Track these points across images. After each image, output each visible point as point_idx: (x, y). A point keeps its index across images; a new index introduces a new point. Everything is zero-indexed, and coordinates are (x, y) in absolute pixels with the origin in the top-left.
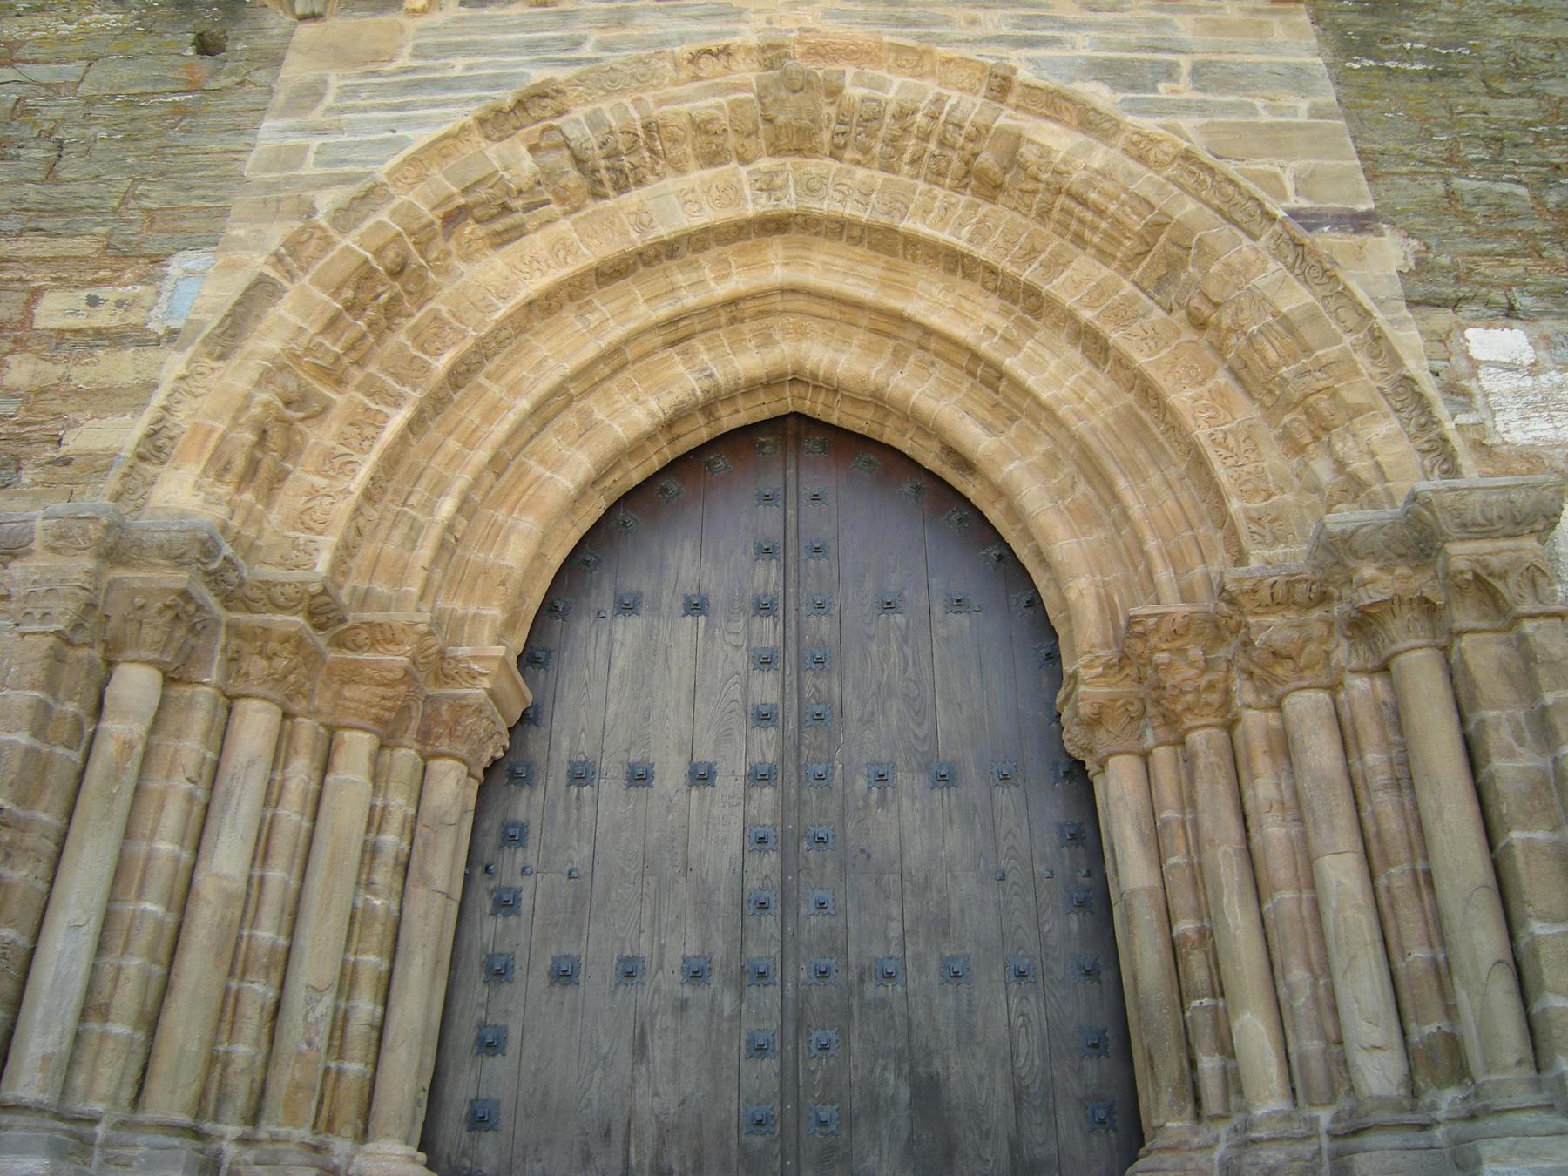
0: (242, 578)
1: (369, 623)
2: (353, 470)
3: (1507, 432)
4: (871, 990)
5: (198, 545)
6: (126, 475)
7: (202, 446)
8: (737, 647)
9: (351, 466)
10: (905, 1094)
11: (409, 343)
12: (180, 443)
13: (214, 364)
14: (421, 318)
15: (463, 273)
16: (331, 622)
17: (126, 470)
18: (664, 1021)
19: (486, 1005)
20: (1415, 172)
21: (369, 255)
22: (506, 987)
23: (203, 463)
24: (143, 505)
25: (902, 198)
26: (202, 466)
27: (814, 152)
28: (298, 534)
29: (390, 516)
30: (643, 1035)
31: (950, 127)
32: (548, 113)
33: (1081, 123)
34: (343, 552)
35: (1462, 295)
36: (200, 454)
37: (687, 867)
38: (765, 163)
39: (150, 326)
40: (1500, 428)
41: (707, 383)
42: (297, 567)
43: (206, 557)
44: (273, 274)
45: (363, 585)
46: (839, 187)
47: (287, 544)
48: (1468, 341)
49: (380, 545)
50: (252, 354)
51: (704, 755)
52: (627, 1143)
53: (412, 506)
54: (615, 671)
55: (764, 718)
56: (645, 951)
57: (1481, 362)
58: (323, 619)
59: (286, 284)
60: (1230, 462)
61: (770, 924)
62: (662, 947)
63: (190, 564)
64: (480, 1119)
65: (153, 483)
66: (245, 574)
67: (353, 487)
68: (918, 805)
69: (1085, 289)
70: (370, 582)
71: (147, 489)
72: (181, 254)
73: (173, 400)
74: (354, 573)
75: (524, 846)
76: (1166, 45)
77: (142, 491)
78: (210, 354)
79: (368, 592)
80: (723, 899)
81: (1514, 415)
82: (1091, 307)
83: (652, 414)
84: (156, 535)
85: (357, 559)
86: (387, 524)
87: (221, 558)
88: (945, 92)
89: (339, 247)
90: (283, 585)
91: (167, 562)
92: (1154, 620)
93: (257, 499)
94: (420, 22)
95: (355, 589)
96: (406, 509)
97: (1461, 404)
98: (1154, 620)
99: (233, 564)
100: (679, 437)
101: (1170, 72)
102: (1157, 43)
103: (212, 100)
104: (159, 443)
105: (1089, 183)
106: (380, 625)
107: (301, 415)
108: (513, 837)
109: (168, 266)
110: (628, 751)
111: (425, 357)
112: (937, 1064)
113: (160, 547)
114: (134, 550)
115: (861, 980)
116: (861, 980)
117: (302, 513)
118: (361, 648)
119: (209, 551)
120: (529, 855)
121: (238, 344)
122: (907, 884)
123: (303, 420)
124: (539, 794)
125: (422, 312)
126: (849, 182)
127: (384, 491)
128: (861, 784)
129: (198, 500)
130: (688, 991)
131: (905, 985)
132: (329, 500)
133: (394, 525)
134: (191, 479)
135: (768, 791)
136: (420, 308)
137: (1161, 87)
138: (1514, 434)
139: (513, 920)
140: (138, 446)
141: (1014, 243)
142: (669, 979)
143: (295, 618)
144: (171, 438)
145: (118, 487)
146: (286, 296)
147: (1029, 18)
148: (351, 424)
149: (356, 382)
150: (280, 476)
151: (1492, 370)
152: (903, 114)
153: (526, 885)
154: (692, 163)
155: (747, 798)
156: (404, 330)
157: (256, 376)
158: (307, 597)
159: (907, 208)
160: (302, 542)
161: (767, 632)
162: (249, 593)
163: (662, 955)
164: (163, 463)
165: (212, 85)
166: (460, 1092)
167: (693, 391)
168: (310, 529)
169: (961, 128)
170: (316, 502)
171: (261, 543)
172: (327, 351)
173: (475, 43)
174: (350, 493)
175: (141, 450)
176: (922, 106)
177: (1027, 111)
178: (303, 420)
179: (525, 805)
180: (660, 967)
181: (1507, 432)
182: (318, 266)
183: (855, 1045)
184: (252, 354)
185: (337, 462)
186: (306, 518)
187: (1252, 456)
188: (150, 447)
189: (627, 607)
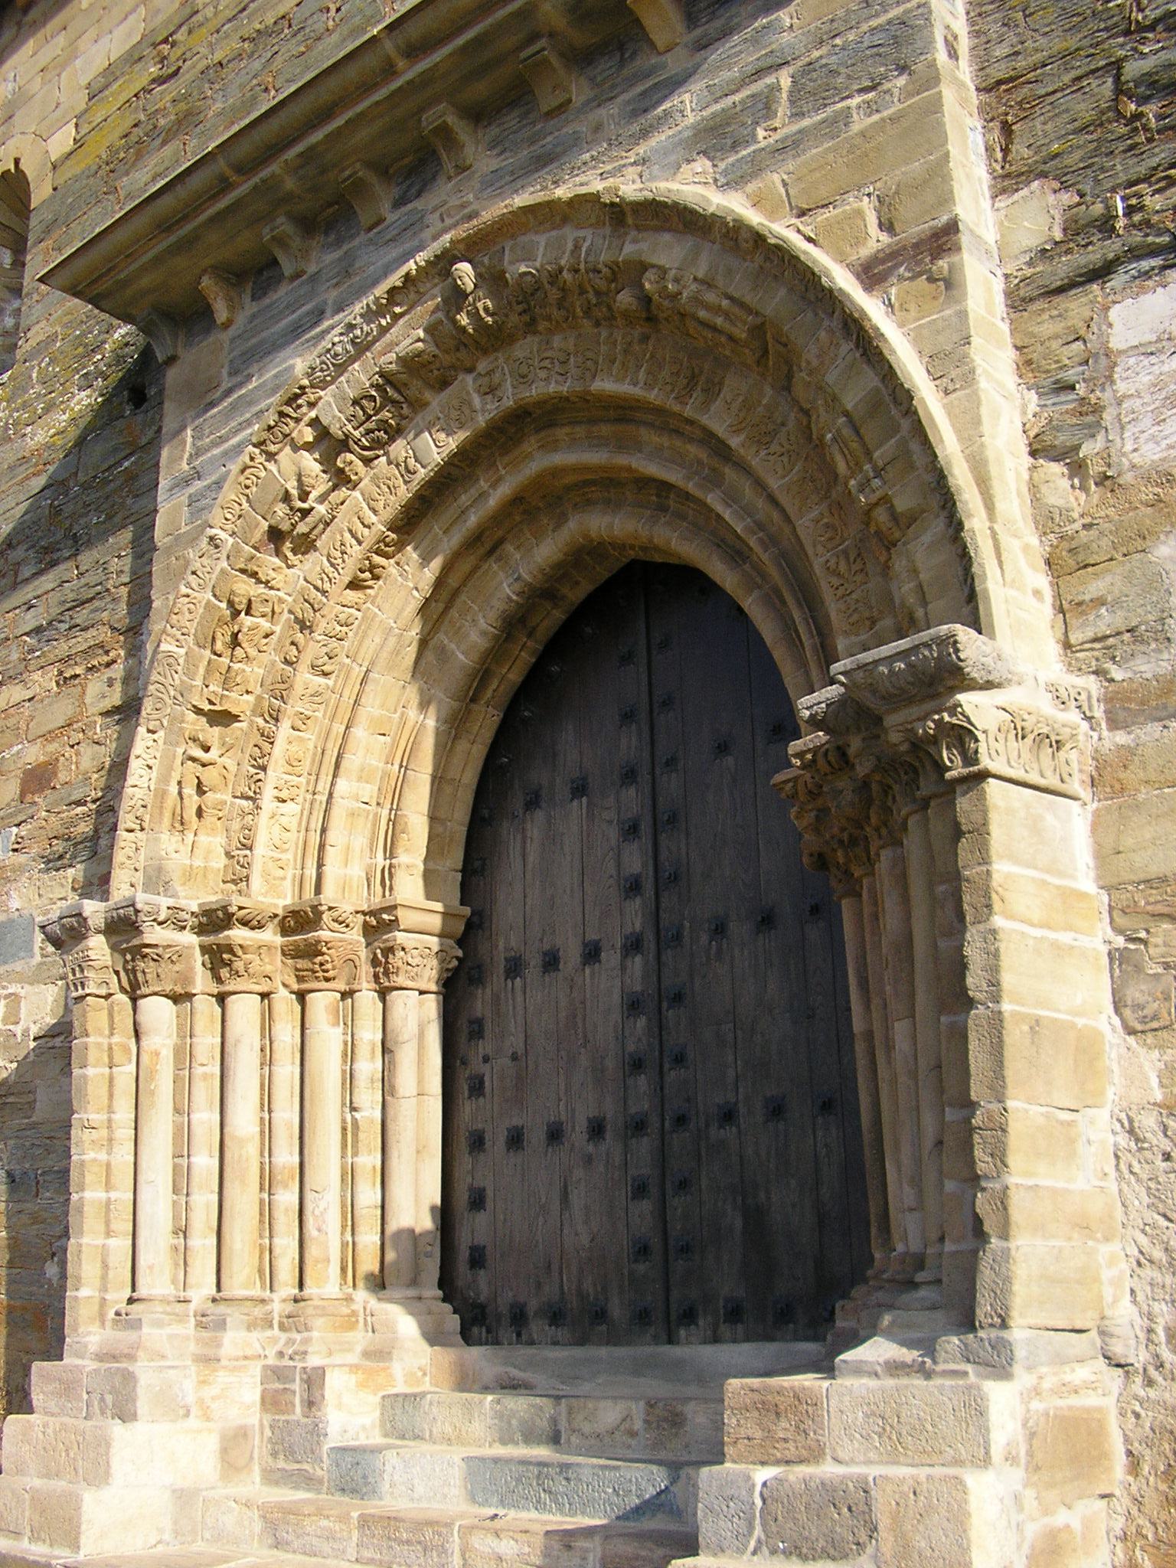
3: (1135, 450)
4: (715, 1133)
8: (610, 822)
10: (738, 1223)
18: (579, 1173)
19: (472, 1172)
20: (1079, 78)
22: (482, 1157)
25: (590, 354)
27: (512, 339)
30: (566, 1187)
31: (591, 275)
32: (304, 409)
33: (685, 226)
35: (1111, 256)
37: (586, 1040)
38: (482, 366)
40: (1129, 447)
41: (517, 587)
46: (542, 364)
48: (1110, 325)
51: (592, 936)
52: (561, 1274)
54: (530, 867)
55: (633, 887)
56: (563, 1118)
57: (1120, 352)
60: (840, 592)
61: (642, 1082)
62: (573, 1110)
64: (477, 1259)
68: (746, 952)
69: (736, 406)
75: (482, 1037)
76: (769, 61)
80: (610, 1063)
81: (1147, 422)
82: (737, 432)
83: (484, 633)
88: (581, 233)
92: (791, 784)
94: (232, 332)
97: (1089, 426)
98: (791, 784)
100: (534, 628)
101: (765, 105)
102: (761, 64)
105: (696, 300)
108: (477, 1031)
110: (541, 940)
112: (762, 1195)
115: (707, 1126)
116: (707, 1126)
120: (484, 1047)
122: (739, 1033)
124: (488, 991)
126: (548, 354)
128: (704, 938)
130: (591, 1148)
131: (738, 1127)
135: (638, 959)
137: (761, 133)
138: (1144, 449)
139: (481, 1099)
141: (678, 374)
142: (577, 1135)
147: (644, 94)
151: (1132, 361)
152: (555, 277)
153: (485, 1069)
154: (428, 395)
155: (623, 968)
159: (596, 363)
161: (632, 799)
163: (573, 1116)
165: (144, 441)
166: (464, 1241)
167: (509, 598)
169: (599, 272)
173: (261, 343)
176: (563, 262)
177: (646, 229)
179: (480, 1004)
180: (573, 1128)
181: (1135, 450)
183: (704, 1183)
187: (859, 578)
189: (533, 802)
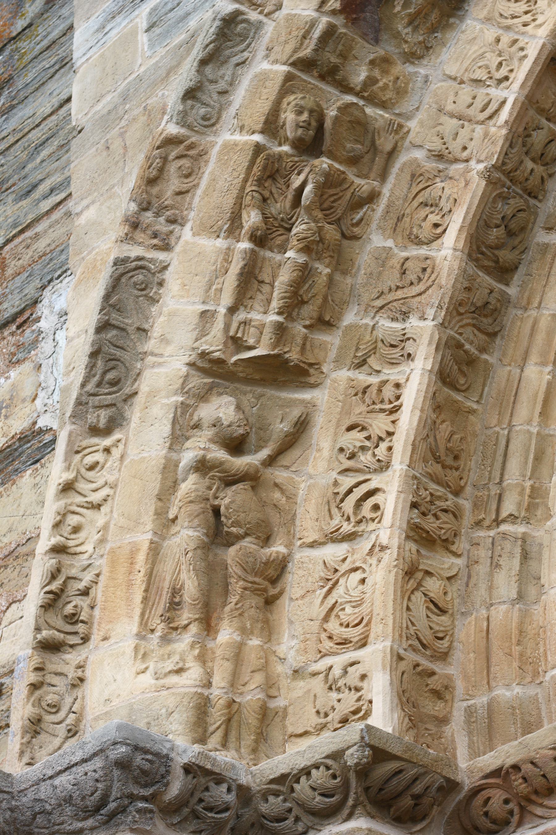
0: (240, 787)
1: (496, 773)
2: (376, 507)
5: (116, 773)
6: (35, 687)
7: (130, 584)
9: (371, 502)
11: (390, 243)
12: (98, 592)
13: (107, 442)
14: (392, 191)
15: (426, 80)
16: (426, 801)
17: (33, 677)
21: (257, 138)
23: (137, 611)
24: (78, 721)
26: (137, 619)
28: (328, 661)
29: (483, 553)
34: (412, 657)
36: (129, 600)
39: (41, 423)
42: (344, 721)
43: (146, 786)
44: (135, 251)
45: (481, 700)
47: (317, 684)
49: (484, 612)
50: (153, 394)
53: (513, 518)
58: (407, 802)
59: (161, 256)
63: (122, 810)
65: (82, 680)
66: (244, 779)
67: (384, 539)
70: (490, 689)
71: (79, 693)
72: (47, 292)
73: (66, 530)
74: (460, 686)
77: (68, 700)
78: (95, 431)
79: (490, 707)
84: (57, 781)
85: (458, 655)
86: (482, 569)
87: (179, 772)
89: (214, 153)
90: (308, 773)
91: (90, 823)
93: (243, 631)
95: (470, 712)
96: (504, 527)
99: (208, 773)
103: (24, 45)
104: (69, 609)
106: (516, 767)
107: (264, 453)
109: (38, 320)
111: (423, 251)
113: (69, 800)
114: (40, 820)
117: (326, 618)
118: (507, 823)
119: (144, 772)
121: (127, 390)
123: (271, 461)
125: (391, 179)
127: (456, 514)
129: (147, 679)
132: (358, 576)
133: (495, 565)
134: (129, 644)
136: (383, 176)
140: (38, 629)
143: (352, 824)
144: (85, 593)
145: (29, 710)
146: (168, 275)
148: (350, 428)
149: (332, 354)
150: (271, 572)
156: (374, 226)
157: (167, 429)
158: (352, 776)
160: (337, 672)
162: (264, 808)
164: (86, 639)
168: (344, 642)
170: (340, 590)
171: (280, 703)
172: (261, 328)
174: (383, 548)
175: (45, 633)
178: (271, 461)
182: (197, 199)
184: (153, 394)
185: (349, 504)
186: (333, 626)
188: (59, 623)
